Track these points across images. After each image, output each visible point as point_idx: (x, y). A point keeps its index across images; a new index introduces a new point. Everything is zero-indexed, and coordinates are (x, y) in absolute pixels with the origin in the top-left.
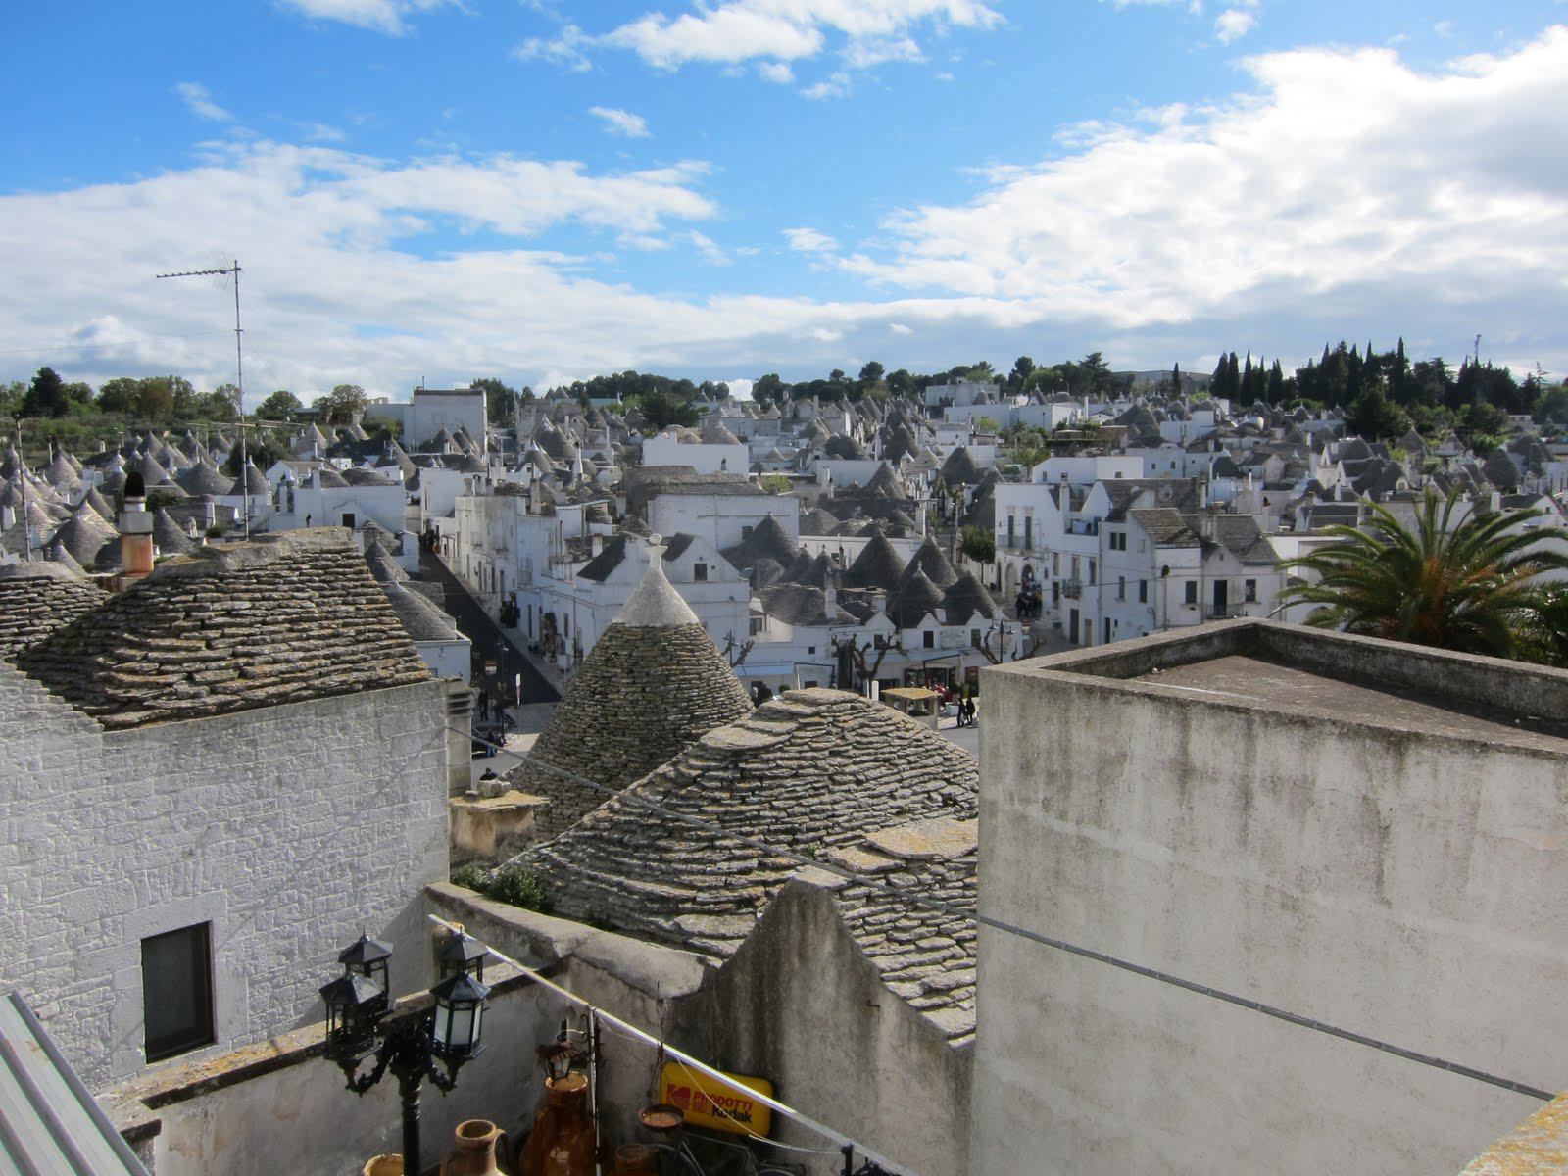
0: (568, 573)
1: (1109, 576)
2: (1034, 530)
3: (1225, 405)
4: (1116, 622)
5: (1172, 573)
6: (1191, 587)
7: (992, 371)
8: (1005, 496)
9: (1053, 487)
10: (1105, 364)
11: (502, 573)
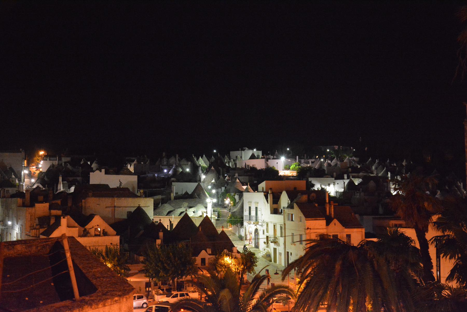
0: (38, 233)
2: (259, 213)
4: (291, 253)
9: (266, 194)
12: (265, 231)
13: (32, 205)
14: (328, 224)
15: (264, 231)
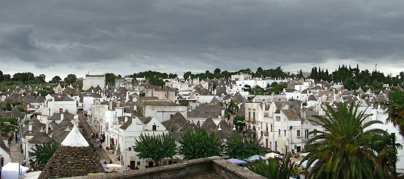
1: (276, 129)
2: (256, 117)
3: (313, 81)
5: (293, 128)
6: (298, 132)
7: (251, 71)
10: (282, 70)
11: (101, 126)
12: (260, 128)
13: (113, 109)
14: (302, 123)
15: (259, 128)
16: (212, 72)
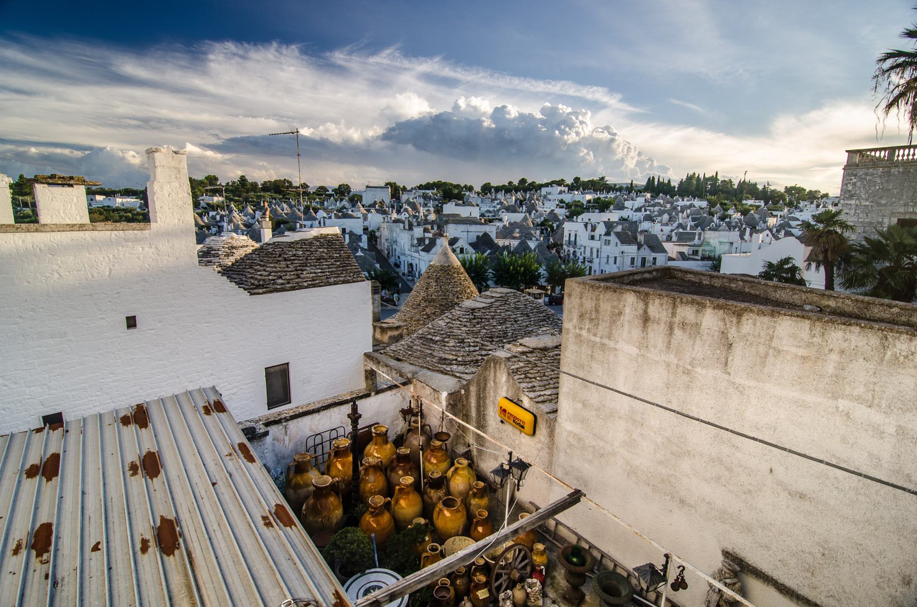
1: (604, 255)
6: (633, 259)
8: (568, 227)
14: (639, 249)
16: (516, 183)
